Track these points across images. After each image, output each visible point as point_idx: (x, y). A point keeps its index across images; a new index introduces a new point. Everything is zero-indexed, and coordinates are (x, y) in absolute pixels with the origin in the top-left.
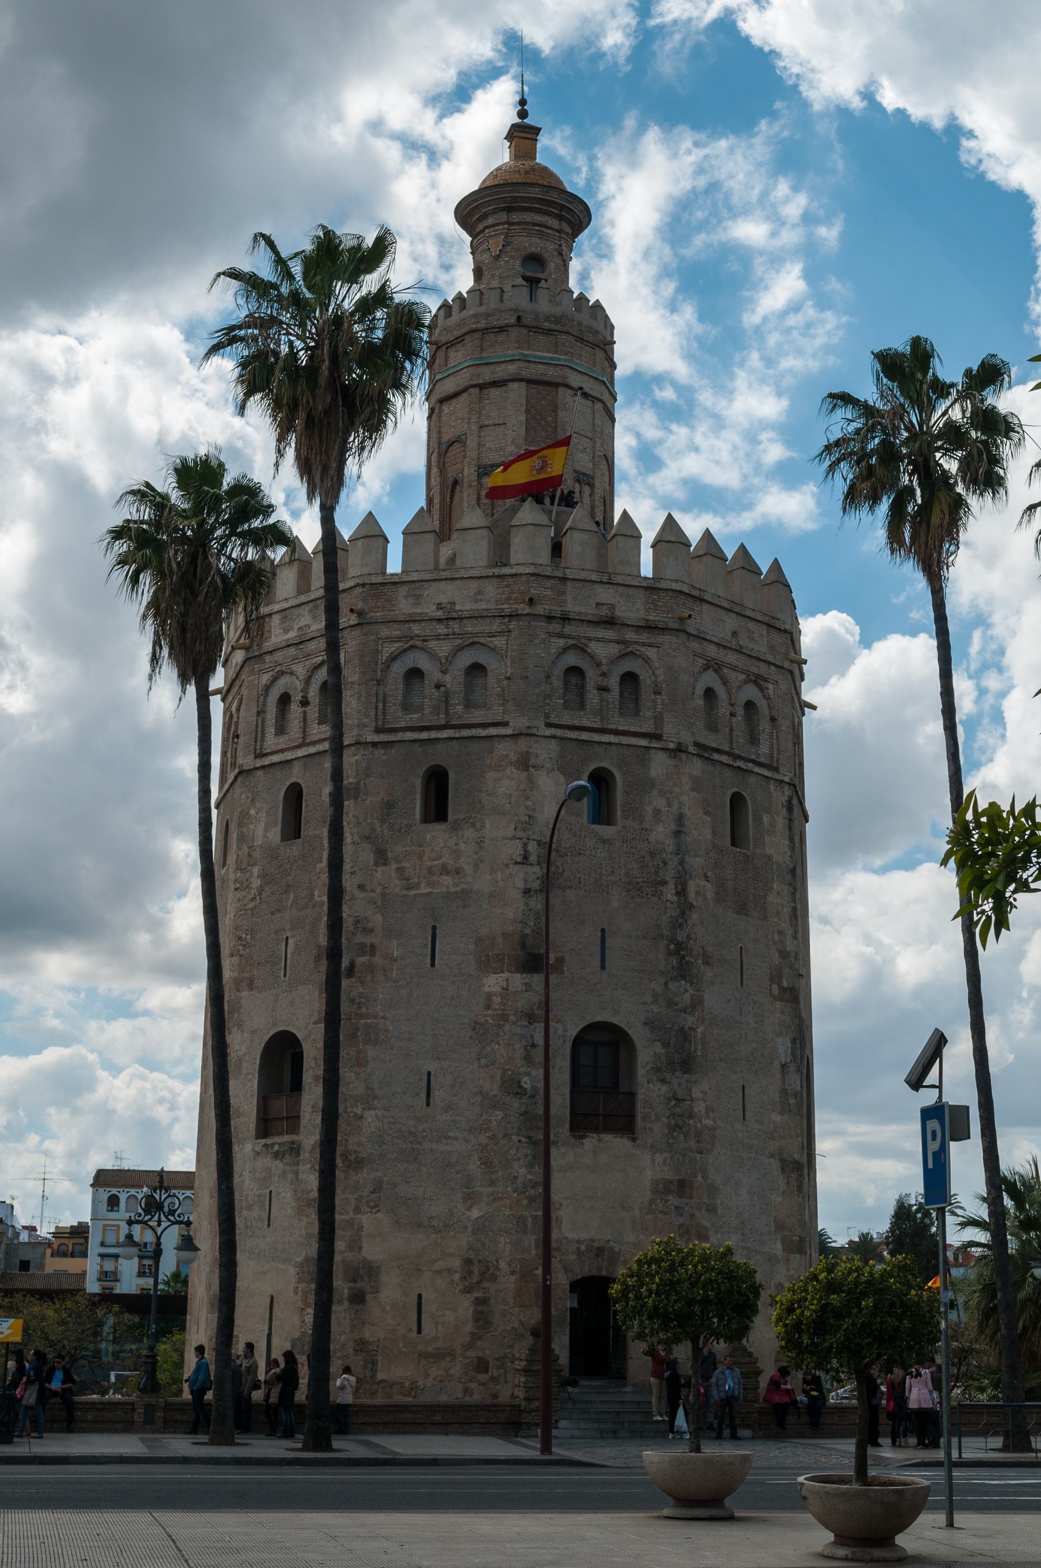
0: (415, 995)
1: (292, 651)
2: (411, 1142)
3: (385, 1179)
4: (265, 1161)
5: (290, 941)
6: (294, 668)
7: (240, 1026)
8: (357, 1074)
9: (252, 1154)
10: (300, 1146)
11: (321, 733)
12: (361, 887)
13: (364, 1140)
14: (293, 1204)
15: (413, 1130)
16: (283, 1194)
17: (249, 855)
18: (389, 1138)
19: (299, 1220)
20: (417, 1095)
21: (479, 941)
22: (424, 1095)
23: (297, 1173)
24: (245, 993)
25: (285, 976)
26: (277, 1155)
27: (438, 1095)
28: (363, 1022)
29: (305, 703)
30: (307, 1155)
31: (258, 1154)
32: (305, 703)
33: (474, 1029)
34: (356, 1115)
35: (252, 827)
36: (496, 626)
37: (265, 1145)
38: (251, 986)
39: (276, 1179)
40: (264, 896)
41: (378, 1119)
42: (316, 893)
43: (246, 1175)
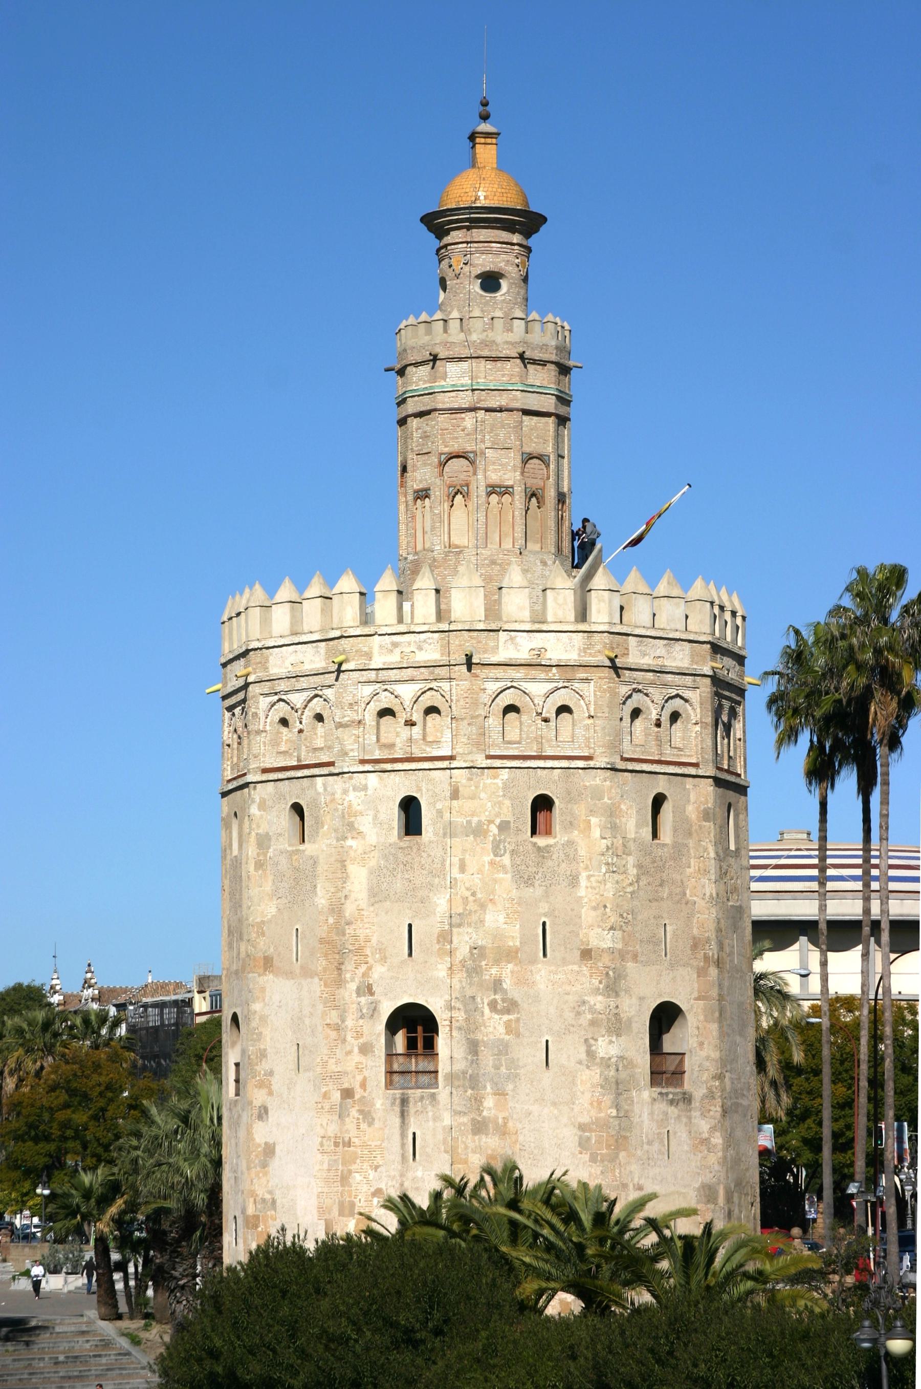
1: (650, 675)
4: (661, 1106)
5: (668, 928)
6: (651, 690)
7: (627, 991)
9: (649, 1100)
10: (691, 1096)
11: (674, 755)
14: (689, 1142)
16: (679, 1134)
17: (624, 846)
19: (694, 1154)
23: (690, 1118)
24: (630, 965)
26: (672, 1102)
29: (658, 725)
30: (698, 1104)
35: (624, 820)
37: (660, 1093)
38: (635, 957)
39: (673, 1121)
40: (641, 883)
42: (688, 892)
43: (645, 1116)
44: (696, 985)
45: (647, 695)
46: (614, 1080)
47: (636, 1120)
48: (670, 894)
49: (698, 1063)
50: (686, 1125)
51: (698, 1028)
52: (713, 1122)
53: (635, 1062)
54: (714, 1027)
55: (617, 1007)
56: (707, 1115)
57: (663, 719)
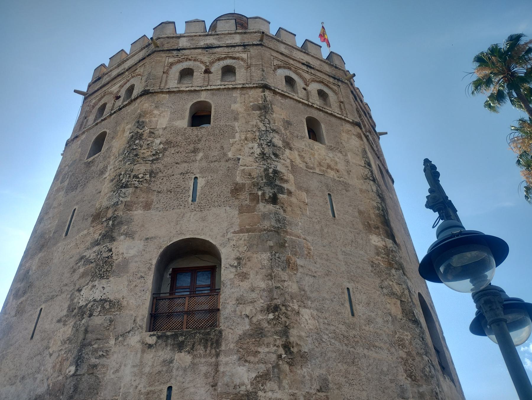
0: (326, 231)
2: (346, 345)
3: (330, 378)
4: (161, 353)
7: (130, 235)
8: (290, 276)
12: (276, 155)
13: (303, 334)
15: (346, 334)
18: (325, 337)
20: (343, 304)
21: (360, 212)
22: (347, 305)
25: (194, 200)
26: (180, 347)
27: (359, 309)
28: (288, 237)
30: (232, 346)
31: (150, 346)
32: (207, 71)
33: (372, 266)
34: (293, 310)
35: (154, 119)
36: (331, 80)
38: (147, 206)
41: (314, 318)
42: (230, 155)
44: (237, 221)
45: (195, 60)
46: (83, 328)
47: (110, 375)
48: (206, 157)
49: (236, 295)
50: (206, 375)
51: (238, 259)
52: (262, 368)
53: (125, 303)
54: (265, 257)
55: (110, 250)
56: (251, 358)
57: (212, 70)
